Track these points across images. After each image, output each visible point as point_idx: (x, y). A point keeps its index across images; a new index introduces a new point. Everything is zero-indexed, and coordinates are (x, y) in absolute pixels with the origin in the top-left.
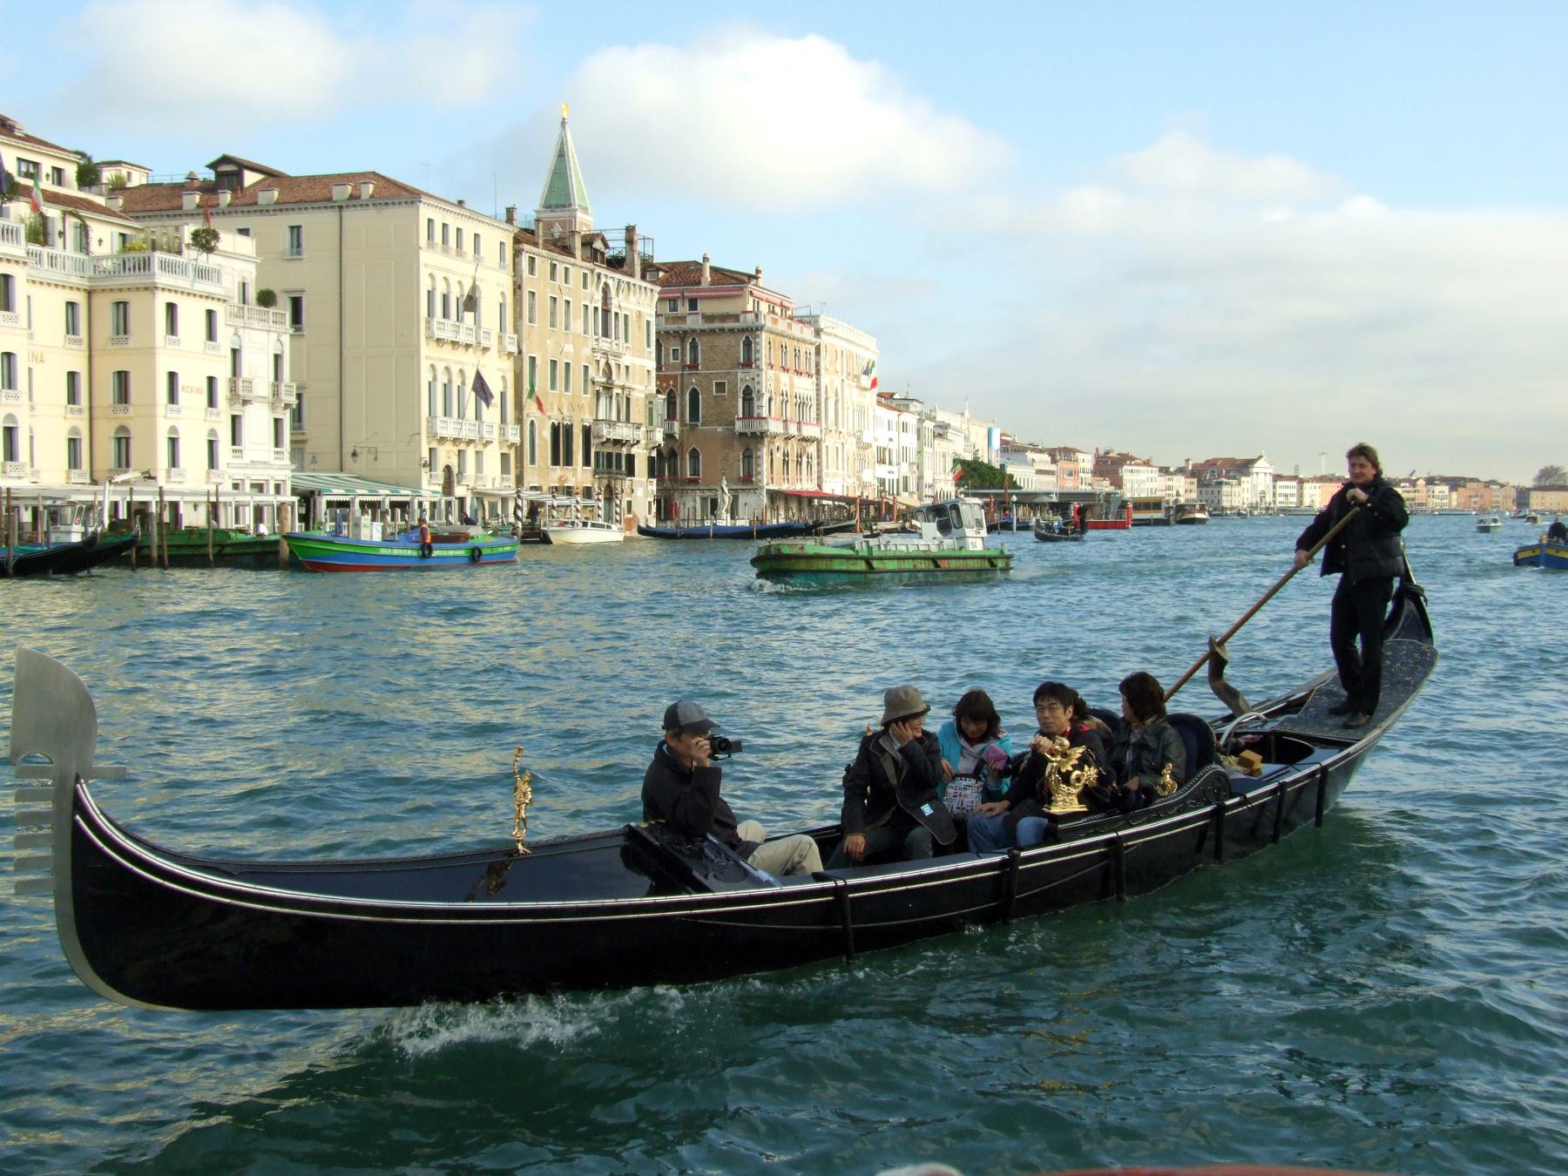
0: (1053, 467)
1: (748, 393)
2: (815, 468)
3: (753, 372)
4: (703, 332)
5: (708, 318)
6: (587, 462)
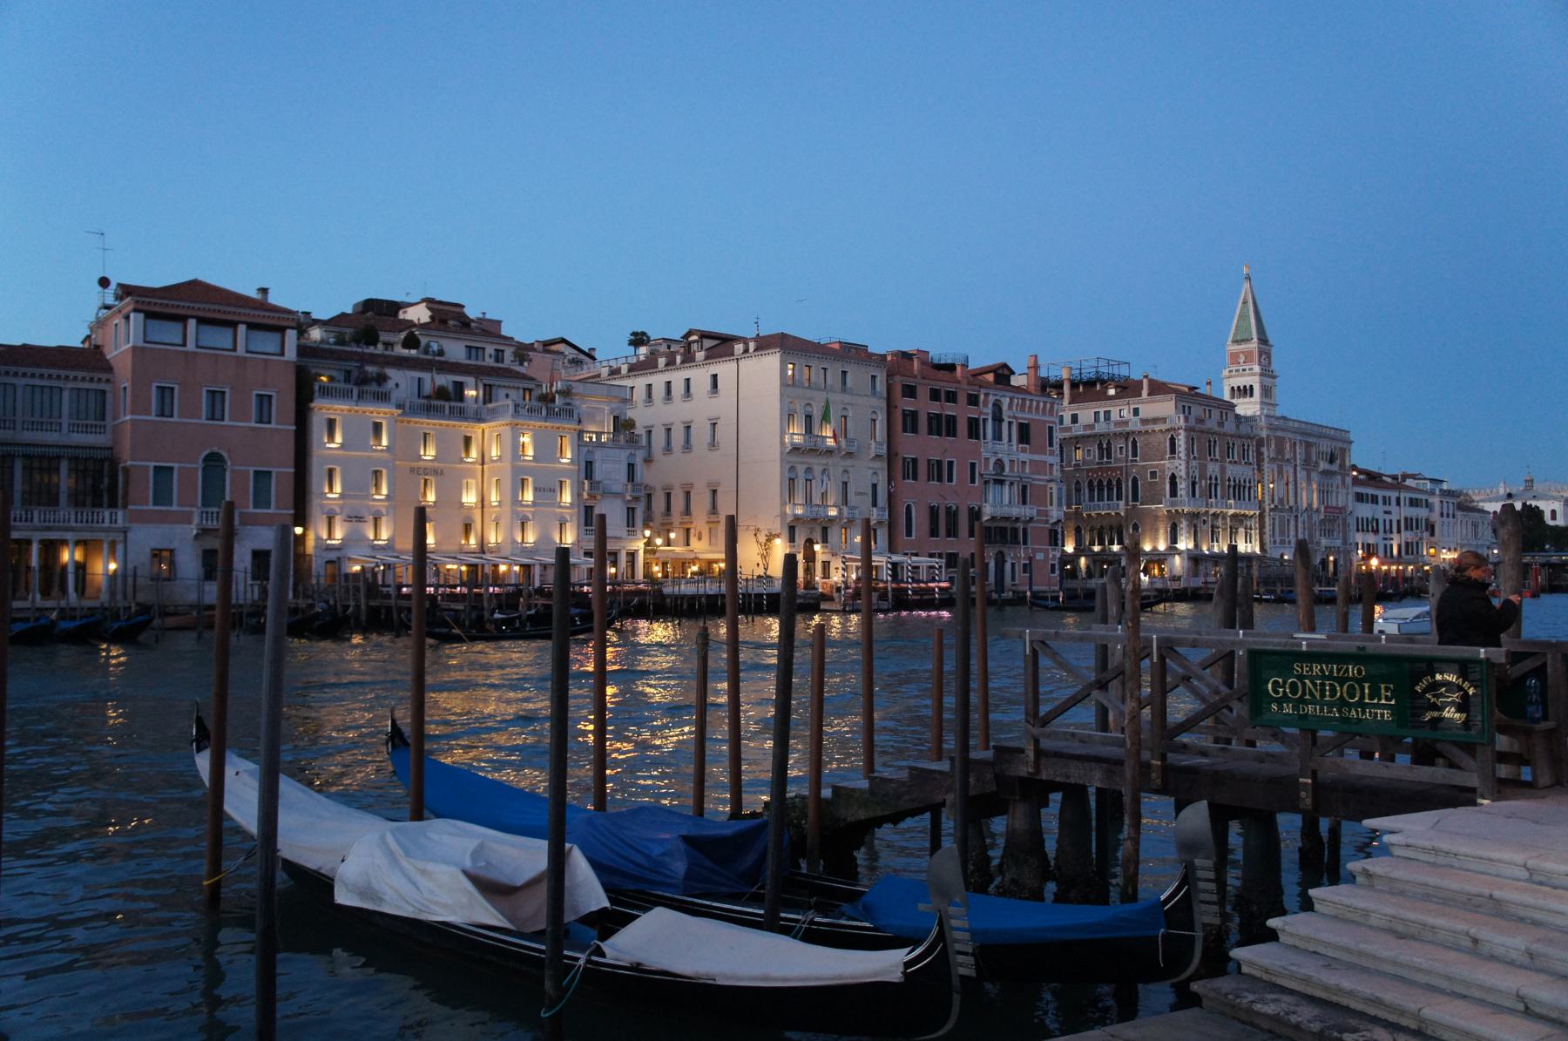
1: (1173, 477)
3: (1177, 462)
5: (1144, 422)
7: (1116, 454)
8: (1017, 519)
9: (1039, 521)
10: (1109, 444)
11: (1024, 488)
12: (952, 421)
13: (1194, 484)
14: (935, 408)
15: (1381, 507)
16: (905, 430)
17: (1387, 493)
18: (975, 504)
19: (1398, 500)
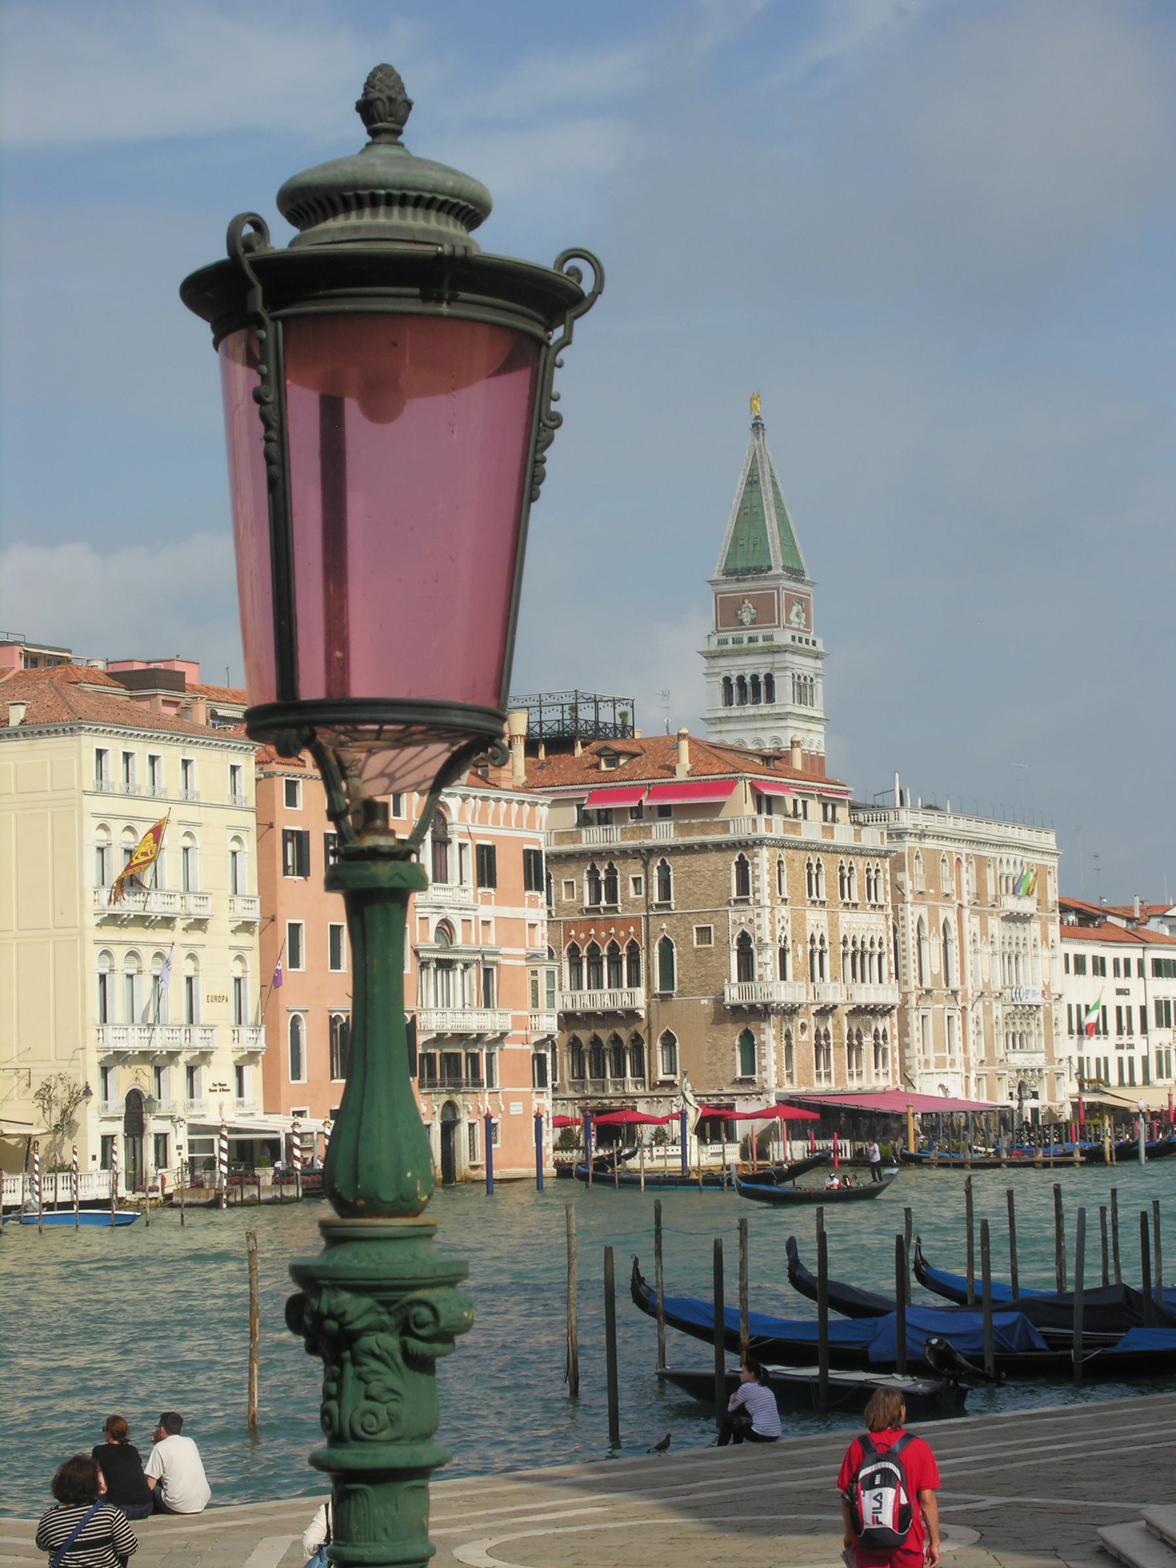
1: (744, 940)
2: (893, 1053)
3: (750, 912)
4: (676, 850)
7: (628, 892)
8: (480, 1036)
9: (515, 1040)
10: (611, 871)
11: (488, 972)
13: (783, 952)
15: (1110, 982)
16: (286, 873)
17: (1122, 953)
19: (1141, 963)
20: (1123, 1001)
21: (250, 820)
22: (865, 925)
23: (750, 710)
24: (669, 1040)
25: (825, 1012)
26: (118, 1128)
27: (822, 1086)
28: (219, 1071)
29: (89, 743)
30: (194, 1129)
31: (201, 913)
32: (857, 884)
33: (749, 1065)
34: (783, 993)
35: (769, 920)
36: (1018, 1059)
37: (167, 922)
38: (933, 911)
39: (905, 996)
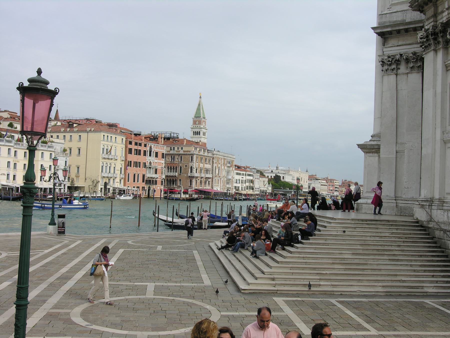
0: (327, 184)
1: (191, 167)
3: (193, 163)
5: (184, 151)
6: (143, 181)
10: (174, 157)
12: (140, 150)
14: (136, 147)
17: (243, 172)
18: (144, 173)
20: (242, 179)
21: (124, 146)
22: (208, 166)
23: (196, 136)
24: (180, 180)
25: (201, 178)
26: (103, 187)
27: (201, 188)
28: (118, 180)
29: (103, 134)
30: (113, 188)
31: (116, 158)
32: (208, 160)
33: (191, 184)
34: (196, 175)
35: (195, 165)
36: (228, 186)
37: (112, 159)
38: (218, 165)
39: (213, 177)
